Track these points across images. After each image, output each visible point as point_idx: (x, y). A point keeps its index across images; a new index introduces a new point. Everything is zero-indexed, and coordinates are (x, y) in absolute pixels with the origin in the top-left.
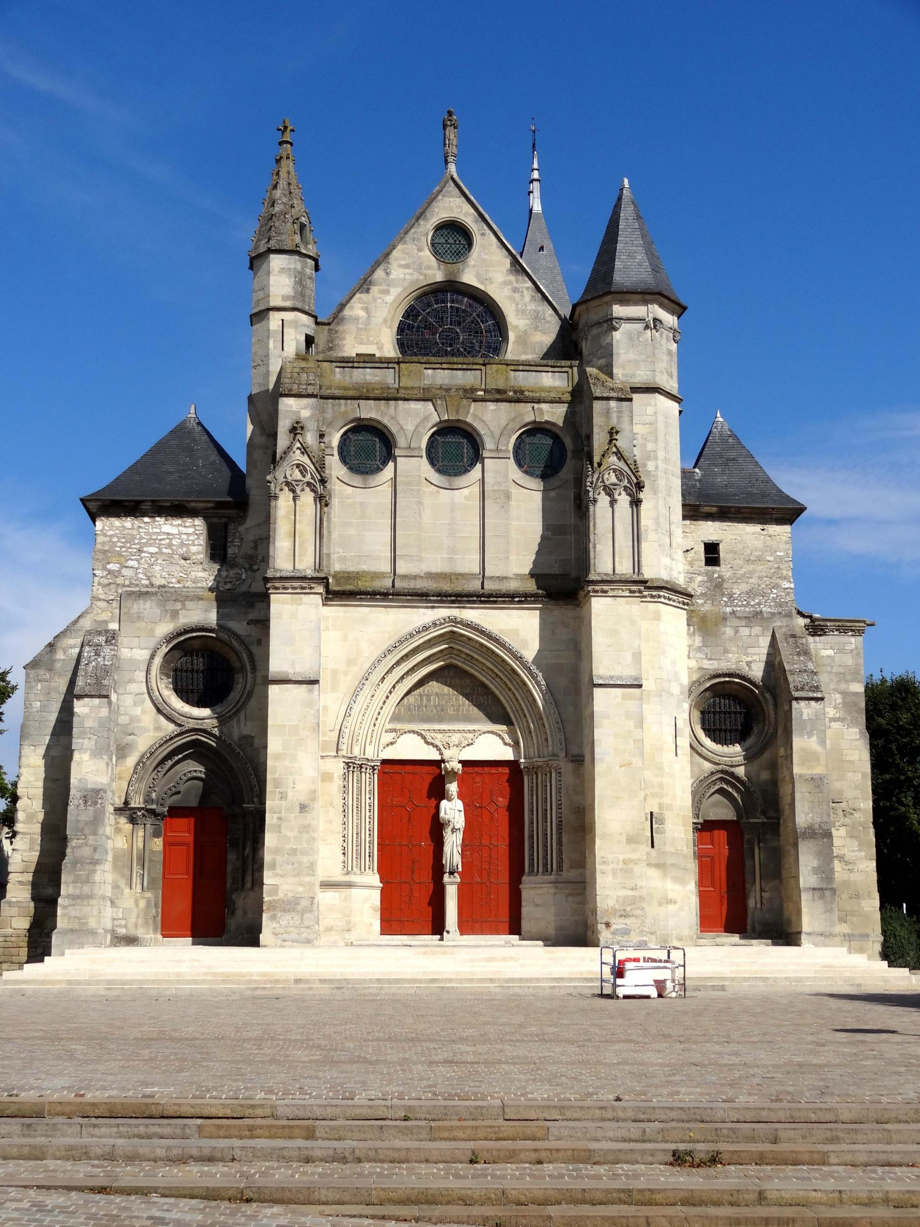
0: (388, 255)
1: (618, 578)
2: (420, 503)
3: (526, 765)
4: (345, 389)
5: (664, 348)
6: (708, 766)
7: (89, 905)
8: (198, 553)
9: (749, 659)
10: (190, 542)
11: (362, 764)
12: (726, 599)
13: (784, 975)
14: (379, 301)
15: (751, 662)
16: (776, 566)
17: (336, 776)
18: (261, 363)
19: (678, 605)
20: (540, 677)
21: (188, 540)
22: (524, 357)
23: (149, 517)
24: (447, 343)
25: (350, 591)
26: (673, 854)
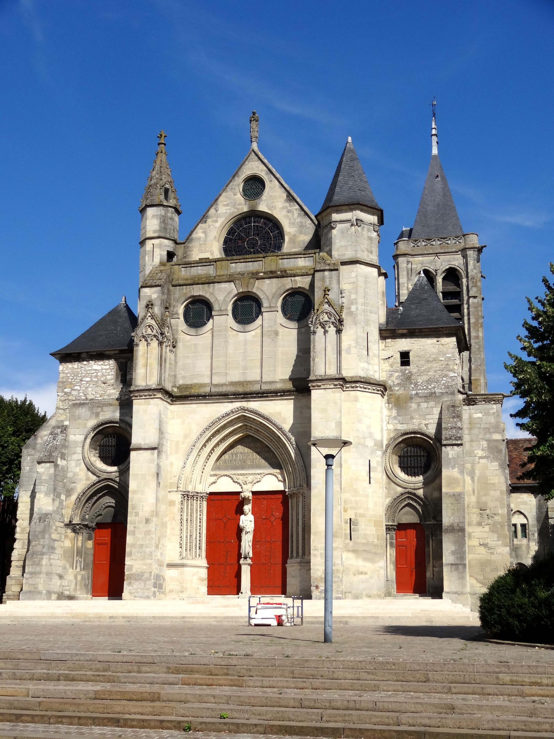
0: (217, 200)
1: (327, 377)
2: (226, 342)
3: (289, 493)
4: (186, 280)
5: (366, 236)
6: (400, 490)
7: (39, 578)
8: (111, 379)
9: (427, 422)
10: (107, 374)
12: (413, 386)
13: (388, 615)
14: (212, 227)
15: (428, 424)
16: (446, 363)
17: (177, 503)
18: (143, 269)
19: (373, 391)
20: (293, 439)
21: (106, 373)
22: (294, 250)
23: (86, 361)
24: (251, 247)
25: (185, 395)
26: (364, 544)
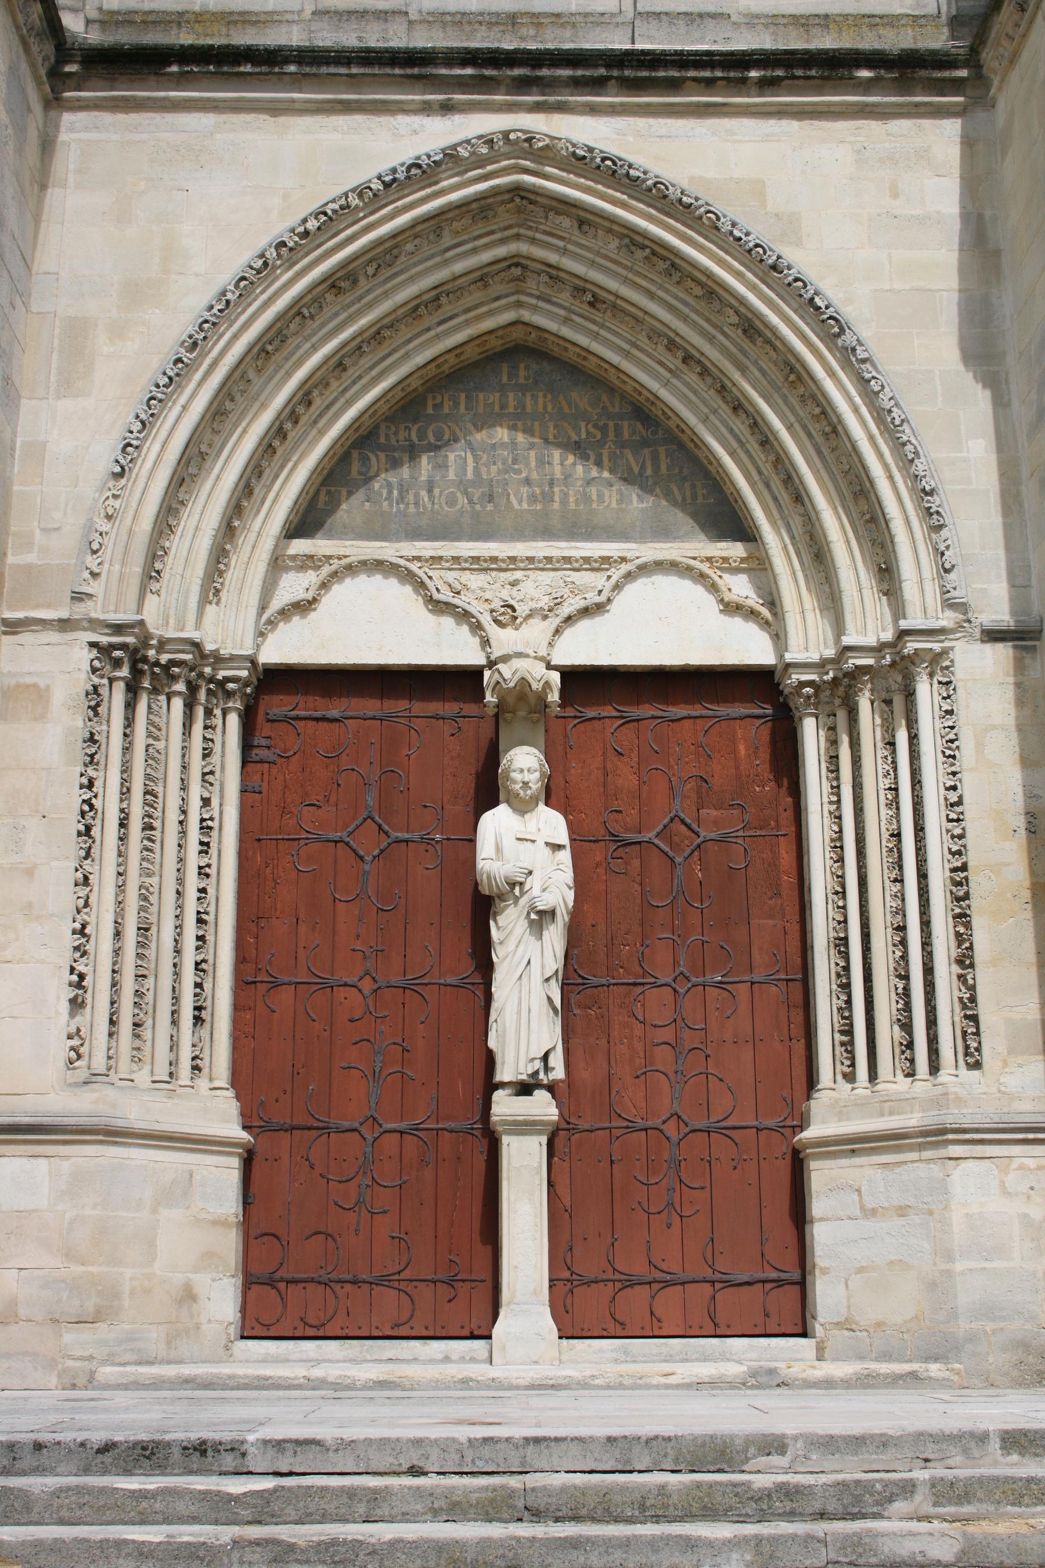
11: (173, 663)
